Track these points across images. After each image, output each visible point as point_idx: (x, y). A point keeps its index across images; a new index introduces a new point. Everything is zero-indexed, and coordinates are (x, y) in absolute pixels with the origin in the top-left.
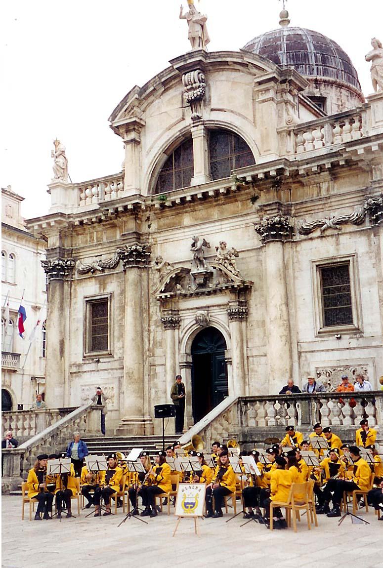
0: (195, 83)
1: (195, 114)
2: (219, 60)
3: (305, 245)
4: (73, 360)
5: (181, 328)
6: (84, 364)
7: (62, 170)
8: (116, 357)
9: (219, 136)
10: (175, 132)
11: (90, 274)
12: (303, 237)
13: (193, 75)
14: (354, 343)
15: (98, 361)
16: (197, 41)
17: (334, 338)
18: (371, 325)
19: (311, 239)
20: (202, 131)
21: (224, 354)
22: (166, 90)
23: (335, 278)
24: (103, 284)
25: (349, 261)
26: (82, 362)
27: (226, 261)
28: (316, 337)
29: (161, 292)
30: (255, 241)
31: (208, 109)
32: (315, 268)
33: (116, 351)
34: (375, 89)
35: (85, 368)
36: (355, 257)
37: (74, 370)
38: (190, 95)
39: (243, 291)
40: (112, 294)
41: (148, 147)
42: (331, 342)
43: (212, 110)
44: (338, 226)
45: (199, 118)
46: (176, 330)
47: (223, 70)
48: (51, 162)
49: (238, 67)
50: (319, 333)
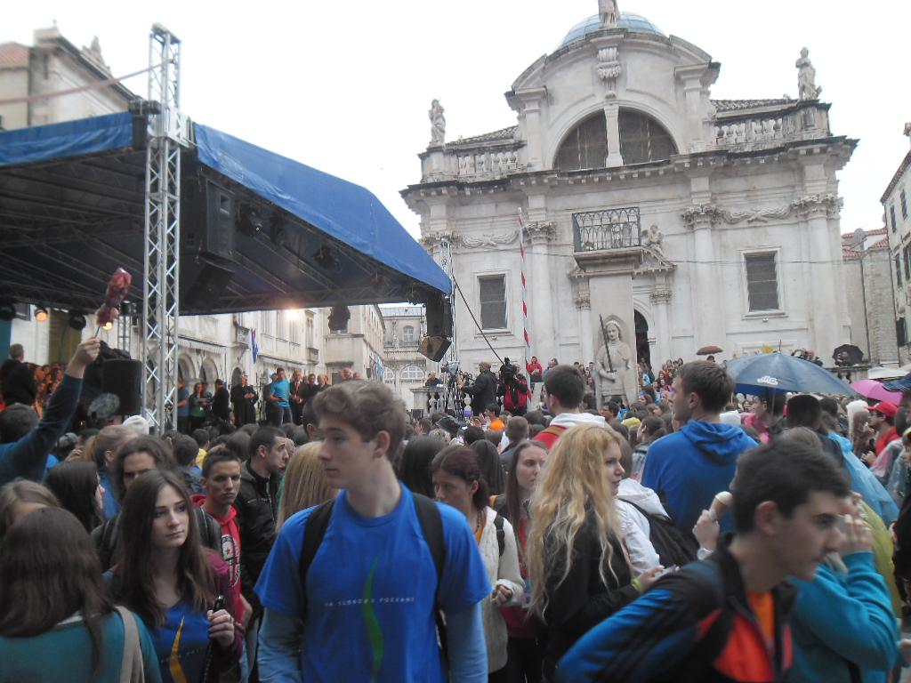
0: (613, 60)
1: (611, 92)
2: (640, 41)
7: (438, 130)
9: (631, 119)
13: (612, 52)
16: (610, 17)
17: (761, 321)
20: (617, 111)
21: (646, 335)
23: (761, 269)
25: (776, 252)
30: (678, 227)
34: (801, 94)
38: (608, 72)
39: (670, 272)
41: (552, 120)
42: (757, 326)
44: (765, 219)
45: (614, 96)
47: (639, 51)
48: (429, 125)
49: (657, 52)
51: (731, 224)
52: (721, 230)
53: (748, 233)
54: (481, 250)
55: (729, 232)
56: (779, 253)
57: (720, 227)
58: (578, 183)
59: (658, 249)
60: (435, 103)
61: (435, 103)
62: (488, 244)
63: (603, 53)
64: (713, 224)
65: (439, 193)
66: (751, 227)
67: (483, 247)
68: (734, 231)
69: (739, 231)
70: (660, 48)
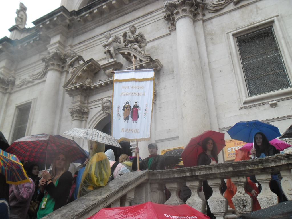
5: (88, 120)
17: (267, 106)
27: (136, 43)
28: (242, 108)
29: (73, 84)
32: (231, 38)
36: (279, 17)
46: (84, 122)
50: (245, 103)
51: (217, 11)
52: (204, 21)
53: (237, 14)
54: (24, 86)
55: (214, 20)
56: (276, 22)
57: (205, 18)
58: (86, 20)
59: (136, 46)
60: (22, 5)
61: (22, 5)
62: (29, 82)
64: (195, 15)
66: (238, 8)
67: (26, 84)
68: (222, 17)
69: (225, 16)
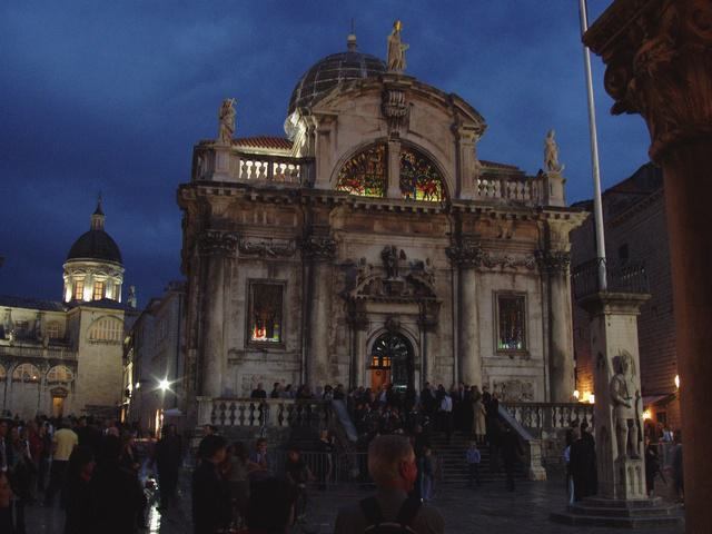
3: (488, 278)
4: (232, 345)
6: (248, 351)
8: (288, 349)
10: (372, 137)
11: (257, 256)
12: (487, 269)
14: (524, 363)
15: (267, 352)
18: (536, 350)
19: (494, 272)
22: (360, 96)
24: (273, 269)
26: (242, 349)
31: (405, 129)
33: (290, 343)
35: (249, 356)
37: (234, 356)
40: (286, 282)
43: (409, 132)
49: (437, 103)
63: (393, 95)
65: (228, 193)
70: (441, 102)
